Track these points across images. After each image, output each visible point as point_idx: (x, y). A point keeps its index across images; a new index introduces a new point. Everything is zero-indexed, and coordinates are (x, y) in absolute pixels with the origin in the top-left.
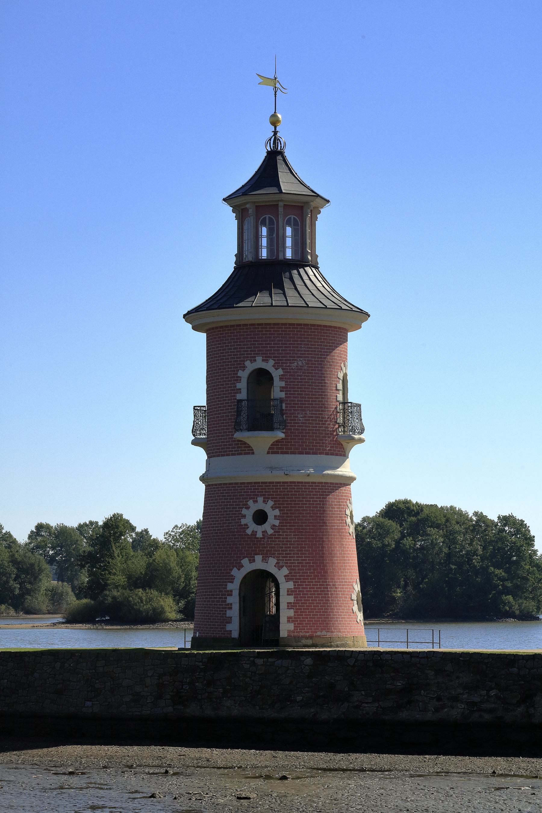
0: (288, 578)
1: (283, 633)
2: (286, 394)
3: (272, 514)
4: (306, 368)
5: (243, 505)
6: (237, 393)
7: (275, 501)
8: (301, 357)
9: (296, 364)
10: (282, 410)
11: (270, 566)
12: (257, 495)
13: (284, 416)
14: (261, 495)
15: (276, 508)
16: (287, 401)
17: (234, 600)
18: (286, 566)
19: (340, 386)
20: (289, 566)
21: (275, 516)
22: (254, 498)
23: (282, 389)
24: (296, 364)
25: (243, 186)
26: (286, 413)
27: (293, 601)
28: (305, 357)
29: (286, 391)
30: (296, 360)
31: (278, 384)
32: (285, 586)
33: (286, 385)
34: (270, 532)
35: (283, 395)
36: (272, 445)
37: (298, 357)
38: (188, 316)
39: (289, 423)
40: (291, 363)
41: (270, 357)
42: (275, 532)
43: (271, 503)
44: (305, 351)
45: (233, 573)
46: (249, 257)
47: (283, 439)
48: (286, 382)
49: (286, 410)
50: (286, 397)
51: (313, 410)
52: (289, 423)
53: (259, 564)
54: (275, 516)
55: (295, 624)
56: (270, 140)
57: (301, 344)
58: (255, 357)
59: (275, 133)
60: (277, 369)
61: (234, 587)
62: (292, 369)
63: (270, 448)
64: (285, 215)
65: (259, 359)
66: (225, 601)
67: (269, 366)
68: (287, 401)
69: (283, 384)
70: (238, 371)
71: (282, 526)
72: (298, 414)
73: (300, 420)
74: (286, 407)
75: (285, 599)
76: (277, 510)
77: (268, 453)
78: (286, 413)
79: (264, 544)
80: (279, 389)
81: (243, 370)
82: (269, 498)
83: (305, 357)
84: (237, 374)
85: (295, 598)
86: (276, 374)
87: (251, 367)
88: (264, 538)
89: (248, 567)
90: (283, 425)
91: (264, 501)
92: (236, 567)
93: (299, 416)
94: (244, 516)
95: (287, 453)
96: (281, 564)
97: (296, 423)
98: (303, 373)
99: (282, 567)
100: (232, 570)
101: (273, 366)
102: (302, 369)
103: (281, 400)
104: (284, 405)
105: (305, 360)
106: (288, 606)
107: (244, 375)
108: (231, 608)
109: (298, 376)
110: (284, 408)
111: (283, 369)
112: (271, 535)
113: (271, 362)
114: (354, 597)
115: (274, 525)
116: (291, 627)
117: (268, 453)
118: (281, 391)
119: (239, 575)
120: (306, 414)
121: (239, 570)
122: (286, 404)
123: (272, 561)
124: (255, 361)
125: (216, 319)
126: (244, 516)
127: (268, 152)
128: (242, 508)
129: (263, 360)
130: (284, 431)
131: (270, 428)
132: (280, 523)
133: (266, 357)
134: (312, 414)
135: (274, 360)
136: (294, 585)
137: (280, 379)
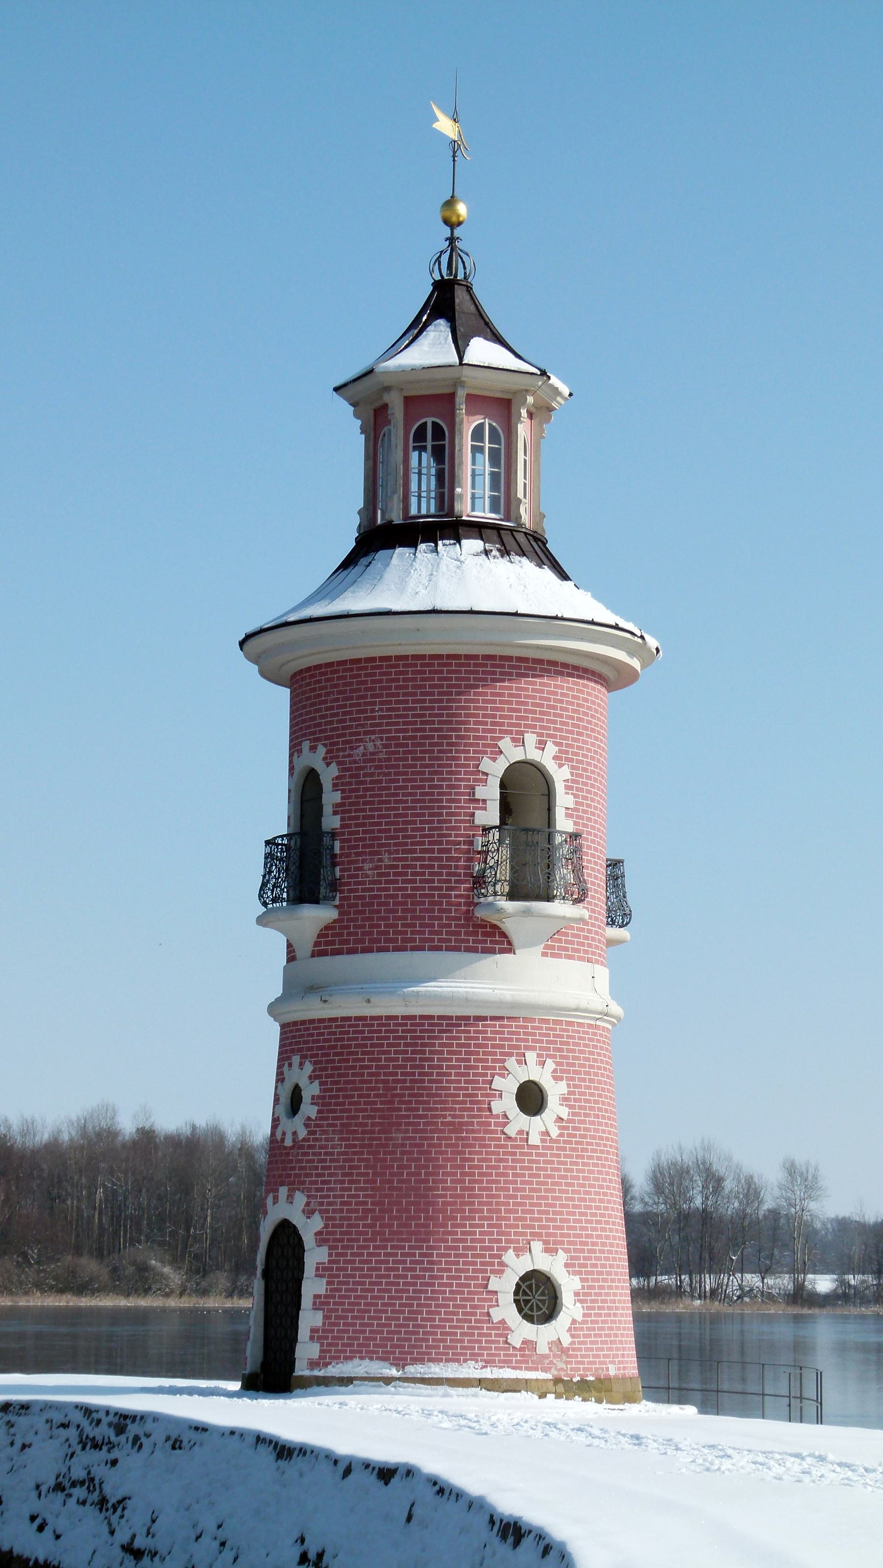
0: (321, 1238)
1: (301, 1370)
2: (342, 819)
3: (311, 1090)
4: (383, 756)
8: (374, 732)
9: (362, 748)
13: (338, 869)
15: (317, 1077)
16: (343, 834)
18: (321, 1212)
20: (327, 1211)
21: (313, 1097)
24: (362, 748)
26: (342, 863)
27: (323, 1292)
28: (381, 732)
30: (361, 740)
31: (331, 798)
32: (315, 1256)
33: (342, 798)
34: (302, 1133)
36: (319, 936)
37: (366, 733)
40: (352, 748)
42: (310, 1133)
44: (381, 717)
47: (335, 921)
48: (343, 791)
49: (341, 855)
50: (342, 826)
51: (397, 852)
54: (313, 1097)
55: (322, 1345)
57: (374, 703)
59: (452, 240)
62: (355, 762)
63: (317, 944)
64: (408, 421)
67: (315, 759)
68: (343, 834)
71: (322, 1119)
72: (364, 861)
73: (367, 876)
74: (342, 848)
77: (313, 956)
78: (342, 863)
79: (291, 1161)
83: (381, 732)
85: (328, 1283)
86: (328, 774)
88: (292, 1147)
93: (367, 866)
96: (312, 1206)
97: (359, 883)
98: (377, 767)
102: (373, 760)
103: (333, 834)
104: (337, 844)
105: (381, 739)
106: (314, 1303)
109: (365, 775)
110: (337, 850)
115: (309, 1118)
117: (313, 956)
118: (335, 813)
120: (380, 860)
122: (342, 841)
123: (300, 1199)
131: (314, 899)
132: (319, 1112)
134: (395, 859)
135: (325, 745)
136: (330, 1255)
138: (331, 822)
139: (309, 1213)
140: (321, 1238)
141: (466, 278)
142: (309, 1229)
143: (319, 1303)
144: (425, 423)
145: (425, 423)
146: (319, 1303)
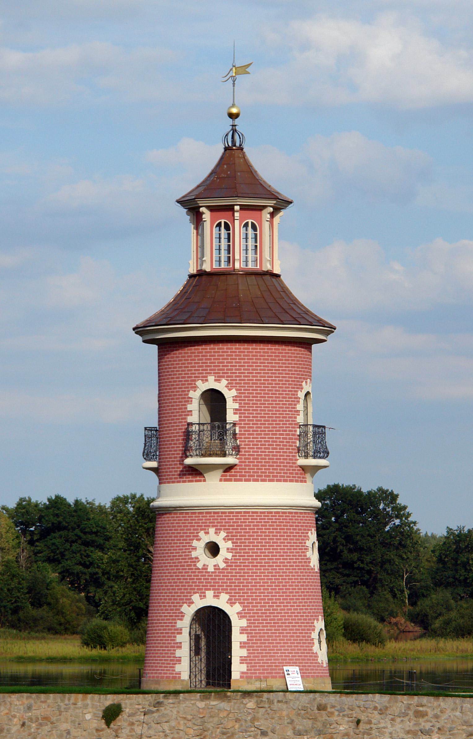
0: (241, 615)
5: (194, 536)
6: (188, 415)
7: (227, 533)
10: (235, 434)
11: (222, 603)
12: (209, 526)
13: (238, 441)
14: (213, 526)
15: (229, 540)
16: (241, 424)
17: (184, 639)
19: (300, 407)
21: (228, 549)
22: (205, 529)
23: (236, 411)
25: (198, 186)
26: (241, 438)
29: (240, 413)
31: (231, 405)
33: (239, 407)
35: (236, 418)
38: (139, 330)
39: (243, 448)
41: (223, 377)
42: (227, 566)
43: (223, 534)
45: (182, 609)
46: (199, 269)
48: (240, 404)
49: (240, 434)
50: (240, 420)
52: (243, 448)
53: (210, 600)
54: (228, 549)
56: (227, 135)
58: (207, 377)
60: (230, 390)
61: (185, 624)
65: (211, 378)
66: (174, 640)
69: (237, 406)
70: (189, 391)
74: (240, 431)
75: (237, 638)
76: (230, 542)
80: (232, 411)
81: (195, 391)
82: (221, 529)
84: (188, 394)
86: (229, 395)
87: (202, 387)
89: (199, 602)
90: (237, 449)
91: (216, 533)
92: (186, 603)
94: (195, 549)
95: (240, 480)
99: (235, 603)
100: (181, 606)
101: (226, 386)
103: (235, 424)
107: (195, 395)
108: (180, 647)
110: (237, 432)
111: (237, 390)
112: (223, 569)
113: (224, 382)
114: (315, 635)
115: (226, 559)
116: (244, 668)
119: (189, 611)
121: (189, 606)
122: (240, 427)
124: (207, 380)
125: (266, 247)
126: (195, 549)
127: (226, 149)
128: (193, 540)
129: (215, 380)
130: (238, 457)
132: (233, 556)
133: (218, 377)
135: (227, 380)
137: (234, 400)
138: (231, 417)
139: (231, 602)
140: (241, 615)
141: (240, 145)
142: (232, 611)
143: (243, 645)
144: (247, 223)
145: (247, 223)
146: (243, 645)
